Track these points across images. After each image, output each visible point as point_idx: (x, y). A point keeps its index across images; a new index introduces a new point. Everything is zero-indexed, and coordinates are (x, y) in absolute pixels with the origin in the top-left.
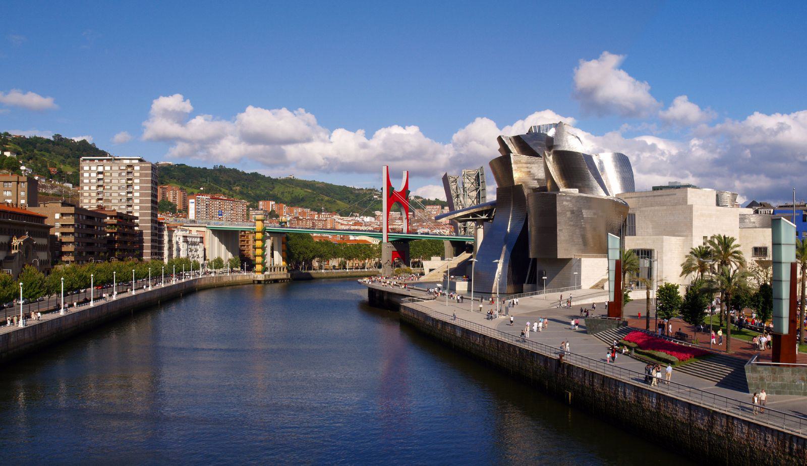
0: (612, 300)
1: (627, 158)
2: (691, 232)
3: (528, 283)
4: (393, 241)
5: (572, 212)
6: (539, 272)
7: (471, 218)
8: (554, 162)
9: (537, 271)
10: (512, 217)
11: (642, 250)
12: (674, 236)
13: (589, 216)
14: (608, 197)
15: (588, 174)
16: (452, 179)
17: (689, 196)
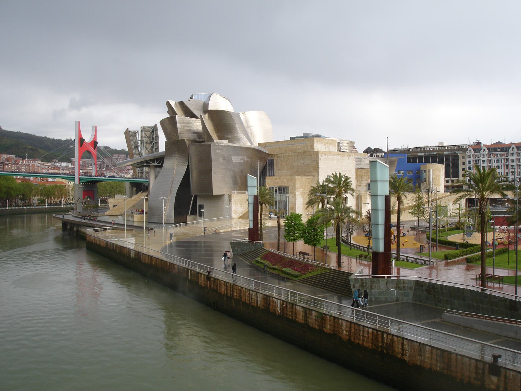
0: (252, 227)
2: (318, 172)
3: (190, 215)
4: (84, 183)
5: (224, 159)
7: (145, 164)
11: (279, 187)
12: (305, 176)
17: (315, 144)
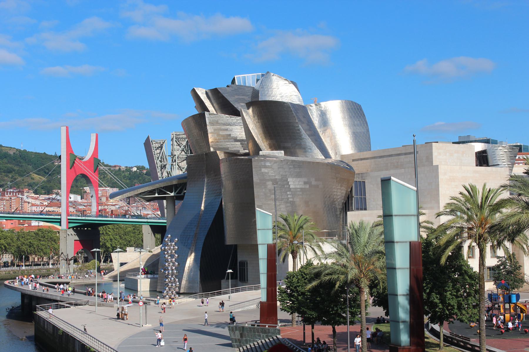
1: (360, 106)
4: (77, 227)
6: (240, 263)
7: (157, 195)
8: (254, 117)
9: (238, 261)
10: (207, 192)
13: (298, 187)
14: (330, 161)
15: (299, 130)
16: (157, 145)
